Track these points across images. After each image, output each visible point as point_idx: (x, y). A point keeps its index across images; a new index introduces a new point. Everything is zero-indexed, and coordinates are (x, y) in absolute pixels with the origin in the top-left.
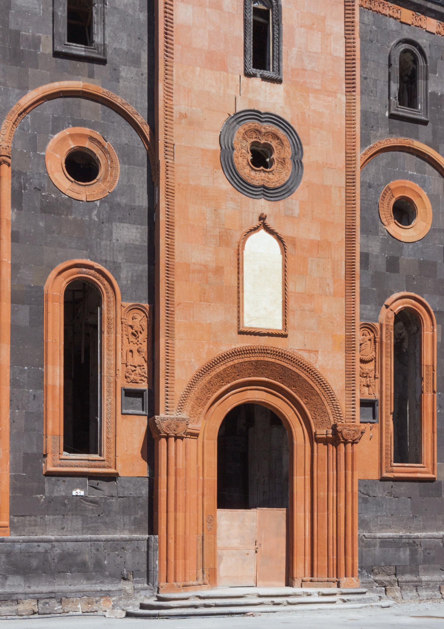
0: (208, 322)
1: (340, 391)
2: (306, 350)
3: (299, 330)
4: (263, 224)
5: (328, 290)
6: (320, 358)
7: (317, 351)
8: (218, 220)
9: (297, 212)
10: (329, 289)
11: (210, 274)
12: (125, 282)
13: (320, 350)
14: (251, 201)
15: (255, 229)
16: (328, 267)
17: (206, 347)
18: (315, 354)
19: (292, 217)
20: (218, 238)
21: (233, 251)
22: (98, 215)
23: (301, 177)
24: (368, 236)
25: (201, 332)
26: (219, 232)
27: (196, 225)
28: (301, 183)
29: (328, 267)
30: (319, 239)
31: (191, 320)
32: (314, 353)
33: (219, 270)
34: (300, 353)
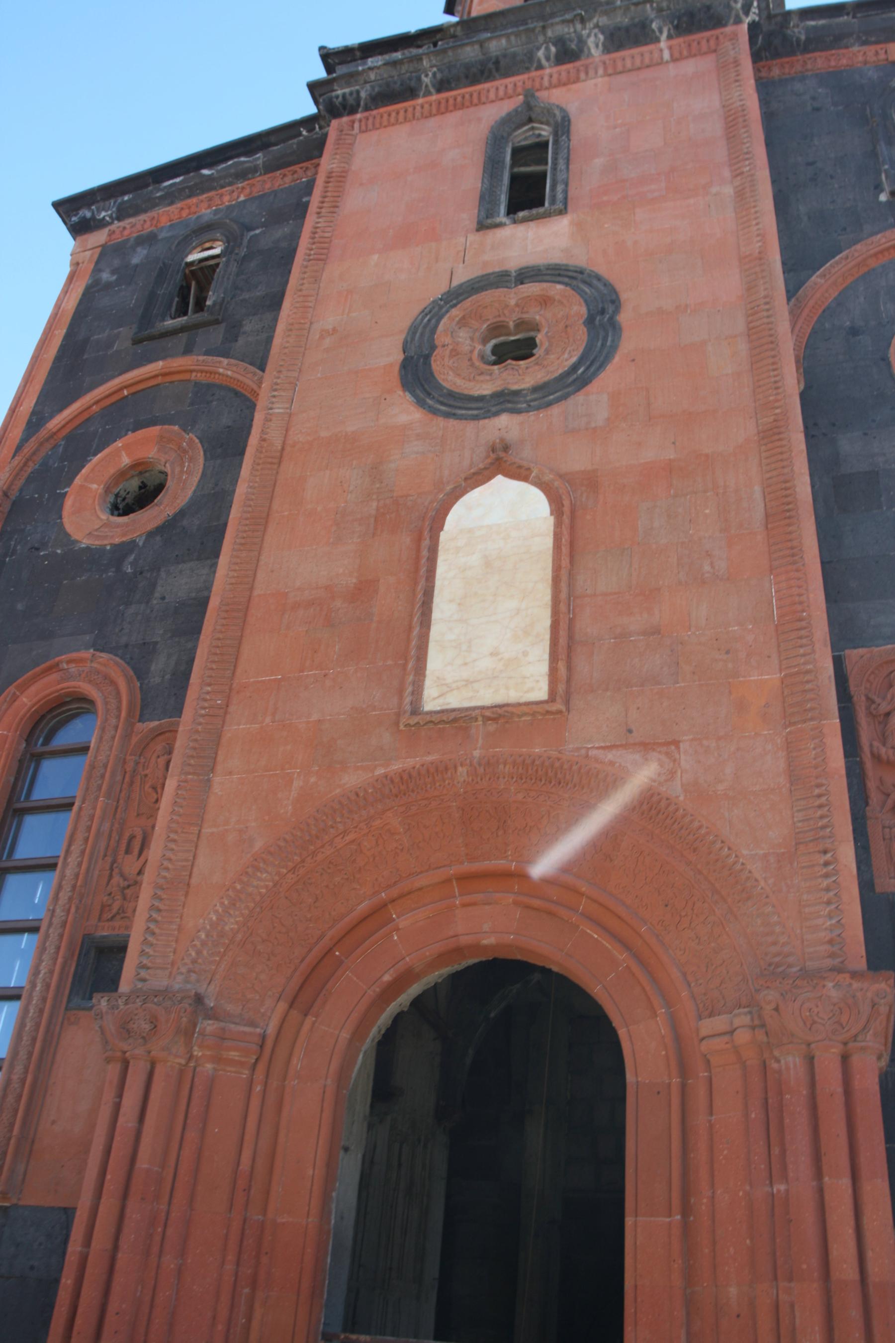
0: (315, 717)
1: (772, 859)
2: (635, 744)
3: (607, 690)
4: (501, 462)
5: (707, 568)
6: (686, 761)
7: (676, 743)
8: (378, 486)
9: (601, 415)
10: (712, 565)
11: (338, 603)
12: (157, 680)
13: (685, 738)
14: (470, 428)
15: (478, 478)
16: (707, 511)
17: (297, 784)
18: (667, 754)
19: (587, 429)
20: (372, 520)
21: (408, 540)
22: (134, 564)
23: (614, 348)
24: (865, 434)
25: (289, 747)
26: (378, 510)
27: (319, 509)
28: (617, 359)
29: (707, 511)
30: (670, 454)
31: (268, 720)
32: (664, 749)
33: (363, 590)
34: (610, 756)
